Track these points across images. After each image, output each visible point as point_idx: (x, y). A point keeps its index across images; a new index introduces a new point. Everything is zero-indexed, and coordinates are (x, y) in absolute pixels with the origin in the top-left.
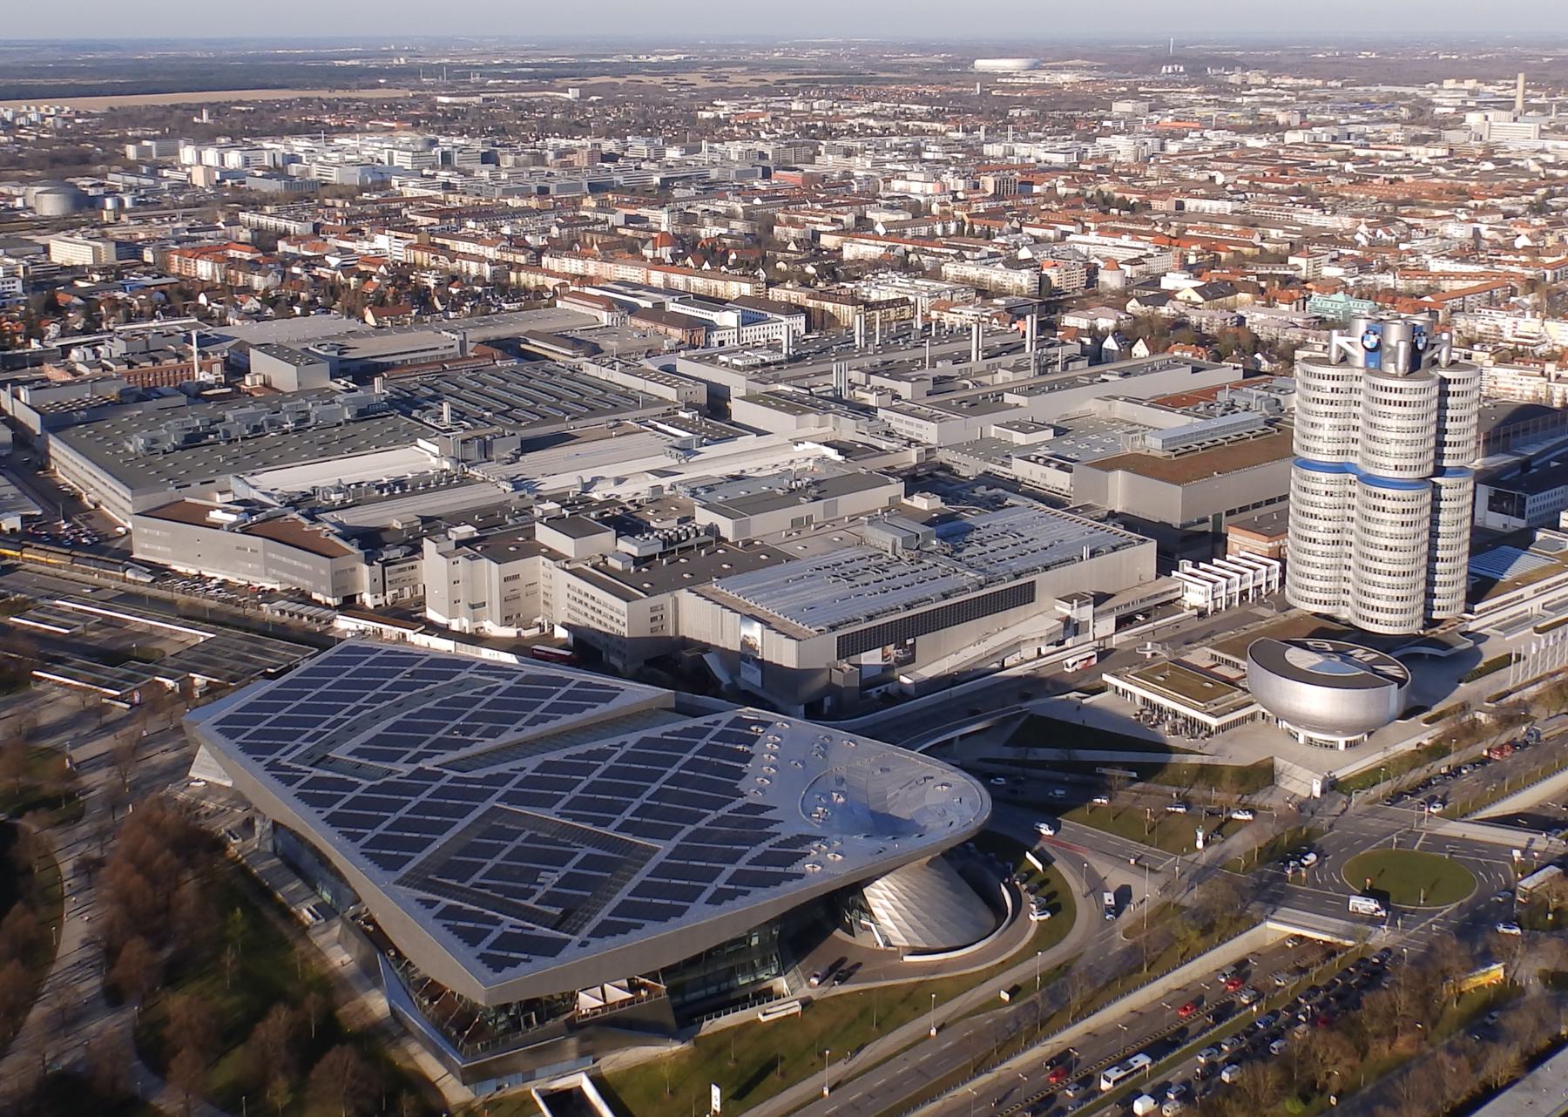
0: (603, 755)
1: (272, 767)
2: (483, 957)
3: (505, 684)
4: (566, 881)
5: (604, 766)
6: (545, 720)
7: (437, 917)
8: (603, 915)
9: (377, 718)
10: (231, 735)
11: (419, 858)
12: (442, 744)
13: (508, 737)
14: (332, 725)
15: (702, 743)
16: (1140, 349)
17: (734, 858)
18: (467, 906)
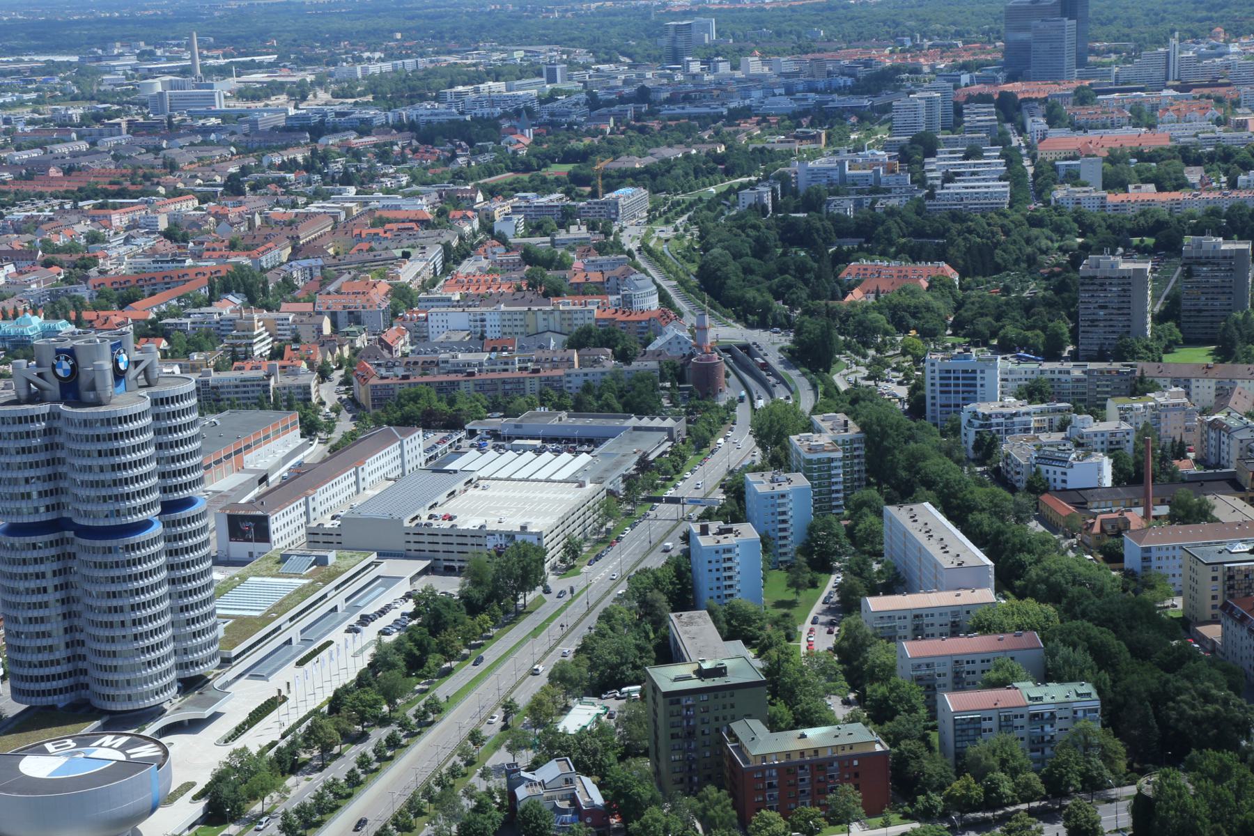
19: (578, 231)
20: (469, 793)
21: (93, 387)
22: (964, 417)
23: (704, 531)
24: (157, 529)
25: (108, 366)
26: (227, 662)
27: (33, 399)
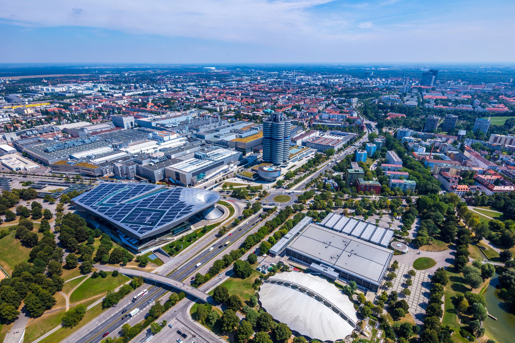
0: (154, 197)
1: (92, 207)
2: (139, 232)
3: (134, 187)
4: (151, 218)
5: (155, 199)
6: (143, 193)
7: (129, 227)
8: (159, 222)
9: (110, 196)
10: (82, 202)
11: (124, 218)
12: (123, 199)
13: (137, 196)
14: (102, 198)
15: (171, 193)
16: (238, 119)
17: (180, 210)
18: (134, 225)
19: (346, 104)
20: (319, 182)
21: (278, 120)
22: (403, 139)
23: (359, 151)
24: (283, 141)
25: (280, 117)
26: (289, 159)
27: (270, 120)
